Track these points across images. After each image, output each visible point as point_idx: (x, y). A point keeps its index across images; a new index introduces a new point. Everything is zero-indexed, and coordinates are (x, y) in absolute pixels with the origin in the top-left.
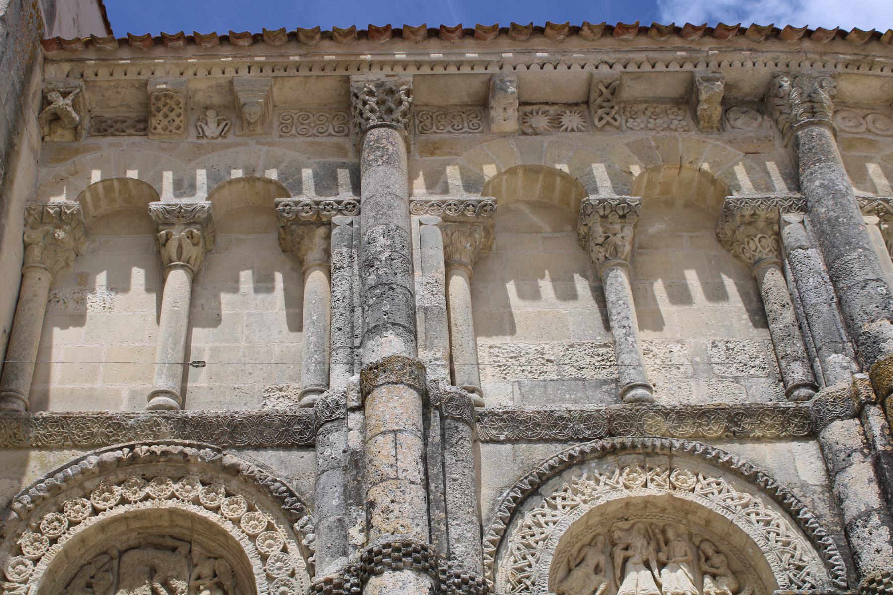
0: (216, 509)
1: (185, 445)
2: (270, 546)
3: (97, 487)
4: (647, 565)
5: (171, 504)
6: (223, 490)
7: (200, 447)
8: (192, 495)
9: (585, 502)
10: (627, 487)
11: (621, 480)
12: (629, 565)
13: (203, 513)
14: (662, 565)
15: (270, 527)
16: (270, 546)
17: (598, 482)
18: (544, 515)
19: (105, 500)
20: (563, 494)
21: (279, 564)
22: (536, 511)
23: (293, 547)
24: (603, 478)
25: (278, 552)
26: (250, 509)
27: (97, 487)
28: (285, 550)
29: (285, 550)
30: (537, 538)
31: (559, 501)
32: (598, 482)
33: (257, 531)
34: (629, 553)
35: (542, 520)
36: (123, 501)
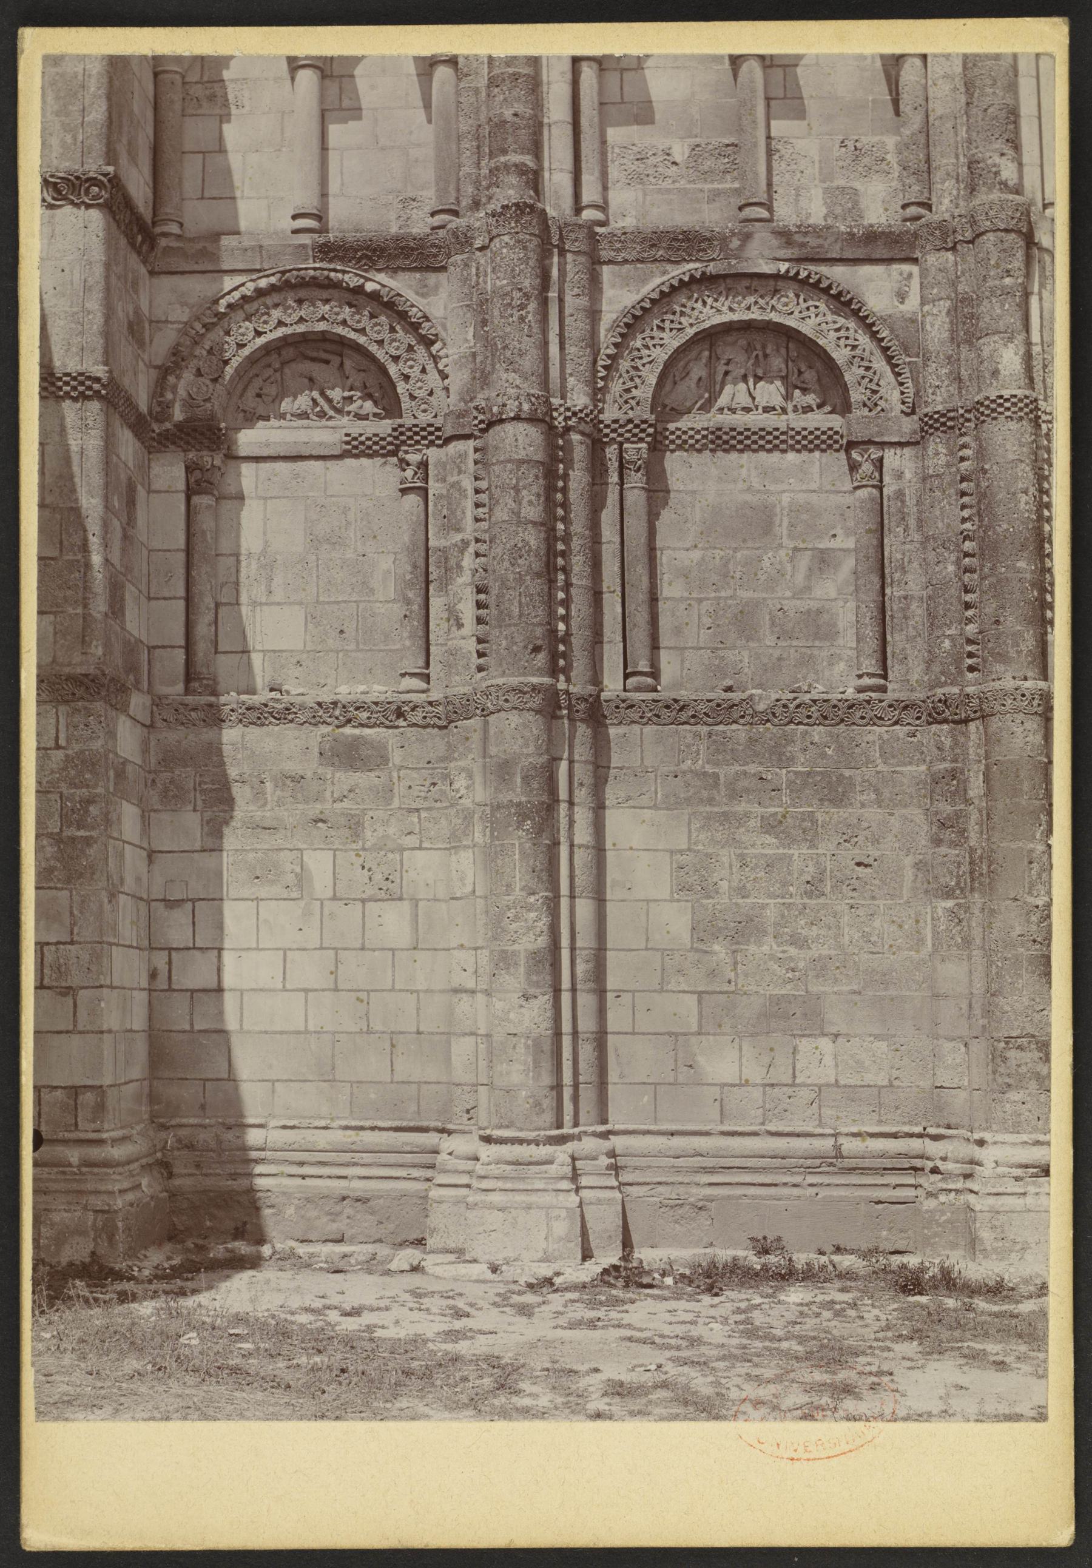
0: (362, 331)
1: (331, 270)
2: (411, 367)
3: (257, 311)
4: (745, 378)
5: (322, 326)
6: (366, 313)
7: (344, 272)
8: (340, 318)
9: (691, 325)
10: (731, 309)
11: (727, 304)
12: (729, 378)
13: (352, 335)
14: (758, 379)
15: (410, 348)
16: (411, 367)
17: (704, 303)
18: (652, 338)
19: (265, 322)
20: (671, 317)
21: (419, 384)
22: (647, 333)
23: (430, 367)
24: (709, 301)
25: (418, 373)
26: (392, 330)
27: (257, 311)
28: (424, 371)
29: (424, 371)
30: (645, 360)
31: (667, 324)
32: (704, 303)
33: (398, 353)
34: (730, 367)
35: (650, 343)
36: (281, 323)
